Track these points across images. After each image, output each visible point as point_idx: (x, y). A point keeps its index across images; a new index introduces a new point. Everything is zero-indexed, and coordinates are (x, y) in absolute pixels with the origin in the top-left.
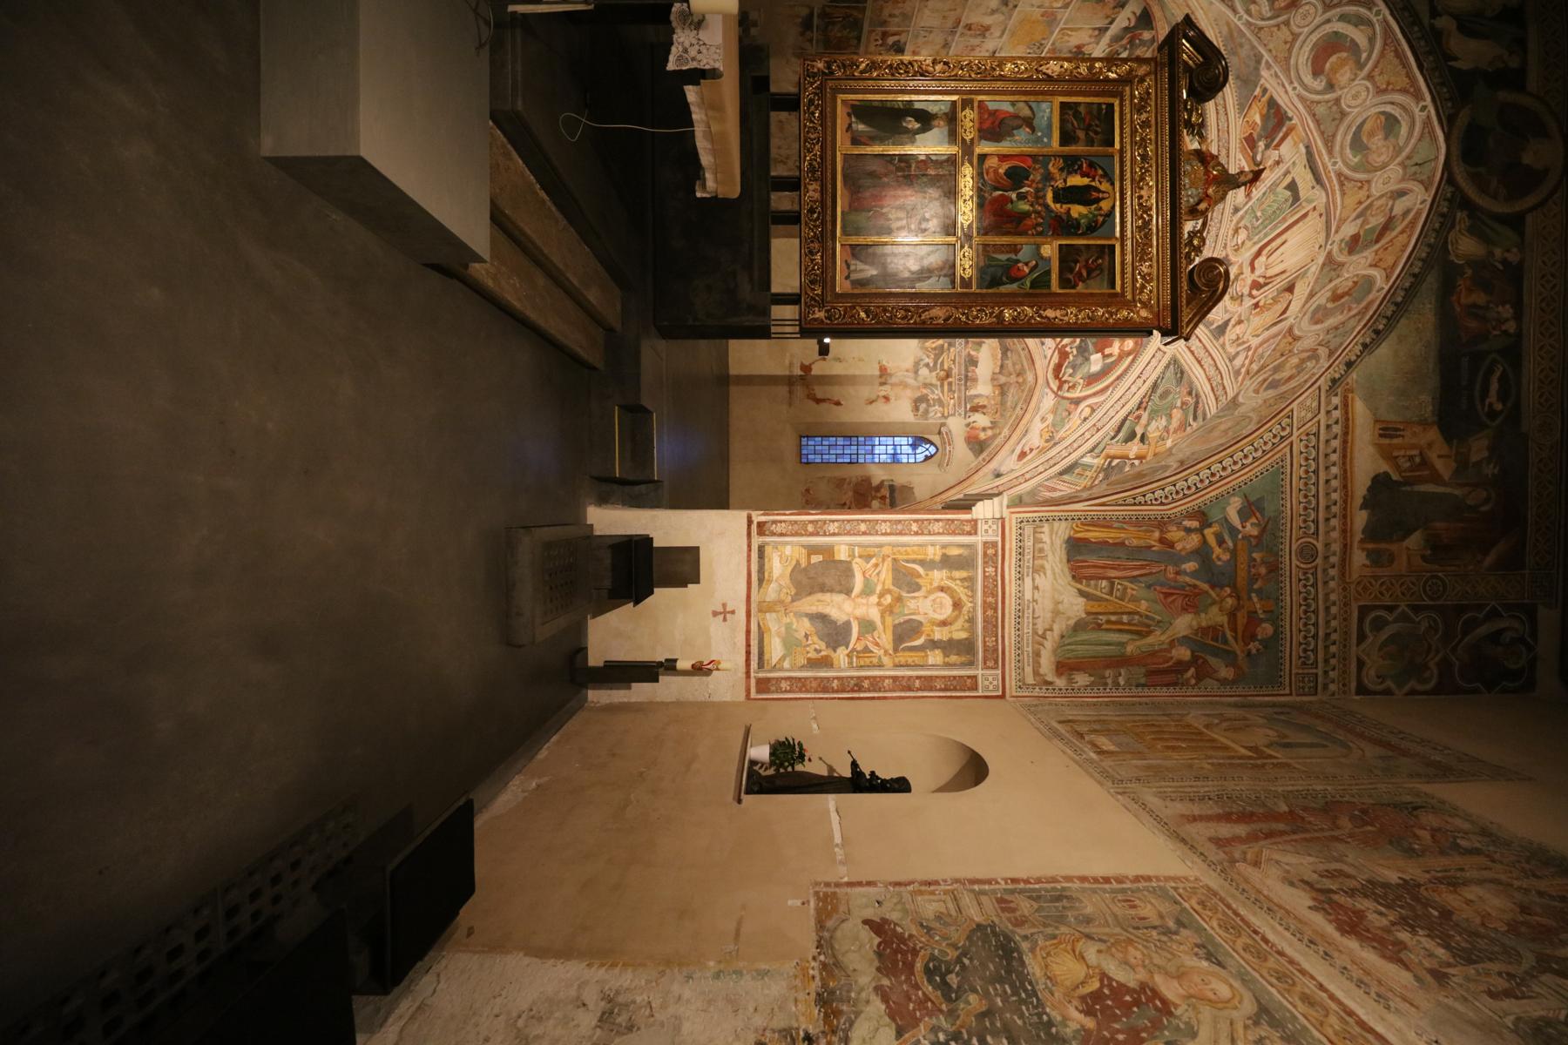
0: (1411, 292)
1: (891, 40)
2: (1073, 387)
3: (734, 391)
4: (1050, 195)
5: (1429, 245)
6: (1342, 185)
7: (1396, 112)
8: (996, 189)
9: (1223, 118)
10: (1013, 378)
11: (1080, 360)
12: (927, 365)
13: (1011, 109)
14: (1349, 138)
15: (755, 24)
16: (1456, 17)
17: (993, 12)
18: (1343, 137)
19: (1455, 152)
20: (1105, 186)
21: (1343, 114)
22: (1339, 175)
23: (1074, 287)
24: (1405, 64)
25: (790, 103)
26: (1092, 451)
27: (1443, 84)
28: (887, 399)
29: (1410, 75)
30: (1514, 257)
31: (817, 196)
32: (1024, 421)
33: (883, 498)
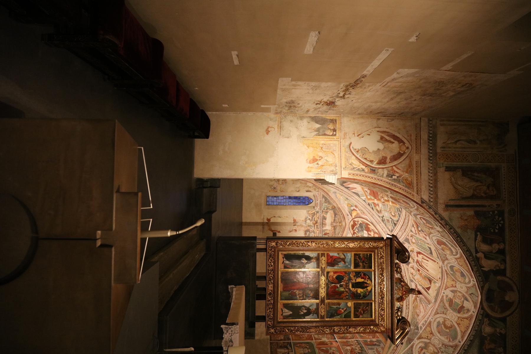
0: (470, 346)
3: (243, 227)
4: (351, 285)
5: (476, 330)
8: (333, 283)
10: (338, 224)
11: (360, 229)
12: (309, 219)
13: (338, 256)
16: (483, 253)
19: (484, 299)
20: (369, 282)
21: (447, 259)
22: (446, 271)
23: (358, 317)
24: (467, 266)
25: (262, 319)
27: (480, 276)
28: (296, 230)
29: (469, 269)
30: (503, 332)
31: (272, 289)
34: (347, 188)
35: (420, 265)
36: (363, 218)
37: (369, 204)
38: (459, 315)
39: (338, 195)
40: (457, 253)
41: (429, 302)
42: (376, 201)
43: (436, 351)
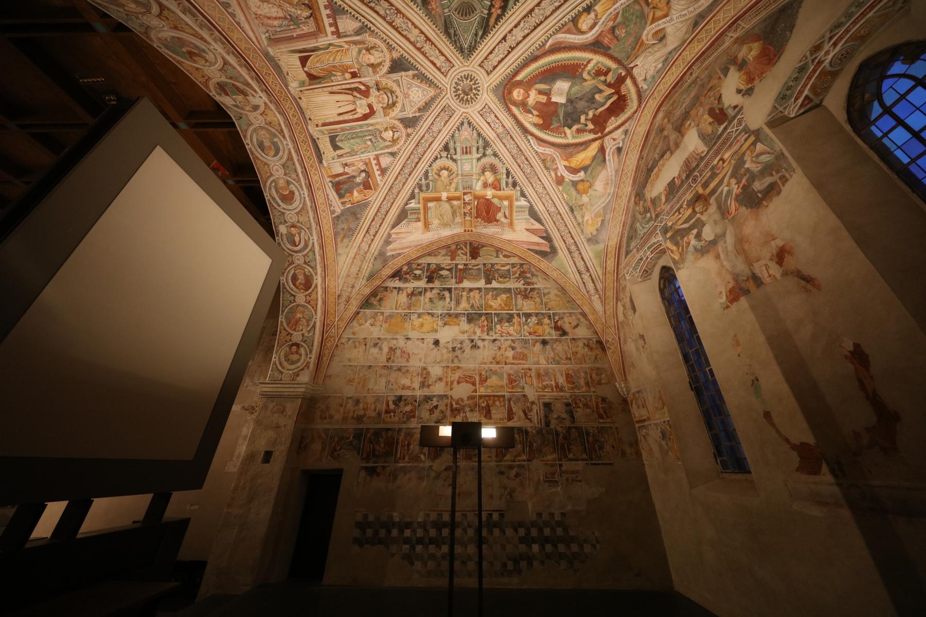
1: (392, 406)
2: (600, 72)
6: (282, 130)
11: (581, 105)
12: (698, 236)
14: (281, 153)
15: (366, 516)
17: (381, 349)
21: (283, 166)
22: (284, 137)
32: (697, 48)
34: (548, 238)
35: (356, 89)
36: (553, 145)
37: (515, 184)
39: (590, 230)
40: (270, 189)
42: (489, 193)
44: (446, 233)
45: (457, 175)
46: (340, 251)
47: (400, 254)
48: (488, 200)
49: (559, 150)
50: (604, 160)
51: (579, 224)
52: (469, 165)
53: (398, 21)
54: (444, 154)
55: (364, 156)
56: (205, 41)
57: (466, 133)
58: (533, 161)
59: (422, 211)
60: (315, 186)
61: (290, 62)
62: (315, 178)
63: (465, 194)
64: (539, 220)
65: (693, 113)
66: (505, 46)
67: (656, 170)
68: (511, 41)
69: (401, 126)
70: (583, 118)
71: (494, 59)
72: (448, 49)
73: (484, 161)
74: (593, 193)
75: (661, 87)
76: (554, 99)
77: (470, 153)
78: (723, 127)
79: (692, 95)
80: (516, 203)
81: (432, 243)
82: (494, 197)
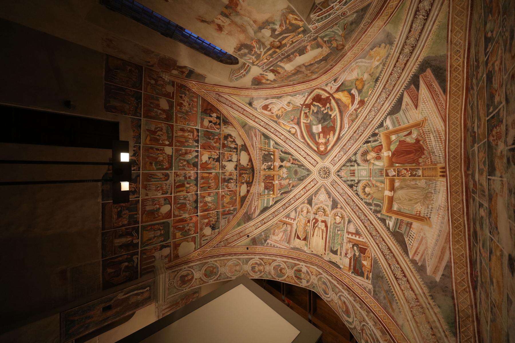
2: (307, 117)
7: (327, 296)
9: (384, 248)
11: (320, 116)
12: (274, 30)
18: (328, 284)
22: (321, 274)
26: (276, 143)
33: (183, 72)
34: (415, 81)
37: (374, 135)
38: (294, 277)
39: (382, 51)
41: (289, 242)
42: (386, 154)
43: (263, 270)
44: (440, 198)
45: (370, 180)
46: (400, 322)
47: (448, 267)
48: (393, 154)
49: (344, 115)
50: (342, 84)
51: (384, 65)
52: (362, 172)
53: (297, 197)
54: (355, 188)
55: (345, 240)
56: (275, 260)
57: (342, 174)
58: (355, 128)
59: (400, 218)
60: (350, 284)
61: (298, 243)
62: (346, 281)
63: (387, 175)
64: (400, 101)
65: (290, 74)
66: (307, 157)
67: (318, 59)
68: (305, 155)
69: (335, 210)
70: (325, 112)
71: (312, 161)
72: (308, 180)
73: (359, 161)
74: (360, 74)
75: (305, 87)
76: (320, 130)
77: (354, 171)
78: (272, 68)
79: (291, 79)
80: (391, 128)
81: (454, 221)
82: (389, 149)
